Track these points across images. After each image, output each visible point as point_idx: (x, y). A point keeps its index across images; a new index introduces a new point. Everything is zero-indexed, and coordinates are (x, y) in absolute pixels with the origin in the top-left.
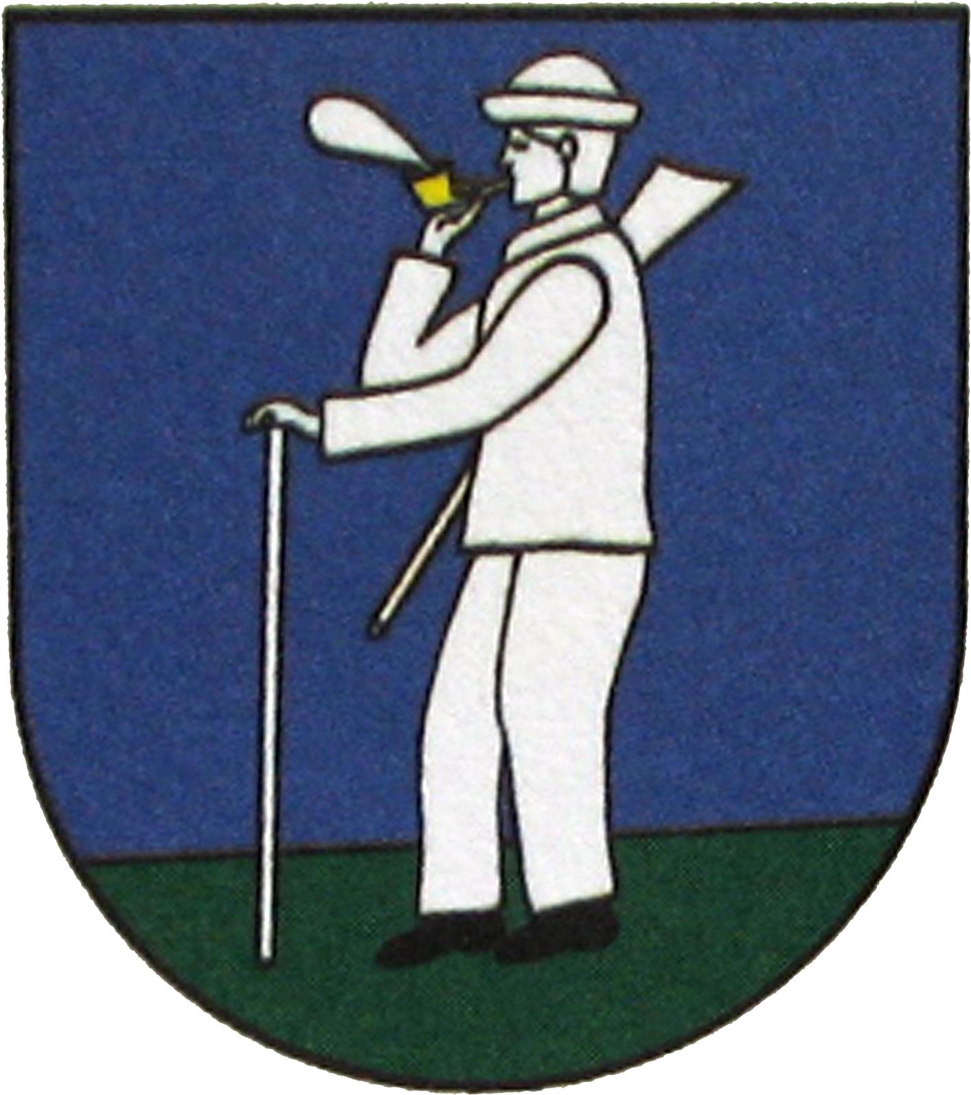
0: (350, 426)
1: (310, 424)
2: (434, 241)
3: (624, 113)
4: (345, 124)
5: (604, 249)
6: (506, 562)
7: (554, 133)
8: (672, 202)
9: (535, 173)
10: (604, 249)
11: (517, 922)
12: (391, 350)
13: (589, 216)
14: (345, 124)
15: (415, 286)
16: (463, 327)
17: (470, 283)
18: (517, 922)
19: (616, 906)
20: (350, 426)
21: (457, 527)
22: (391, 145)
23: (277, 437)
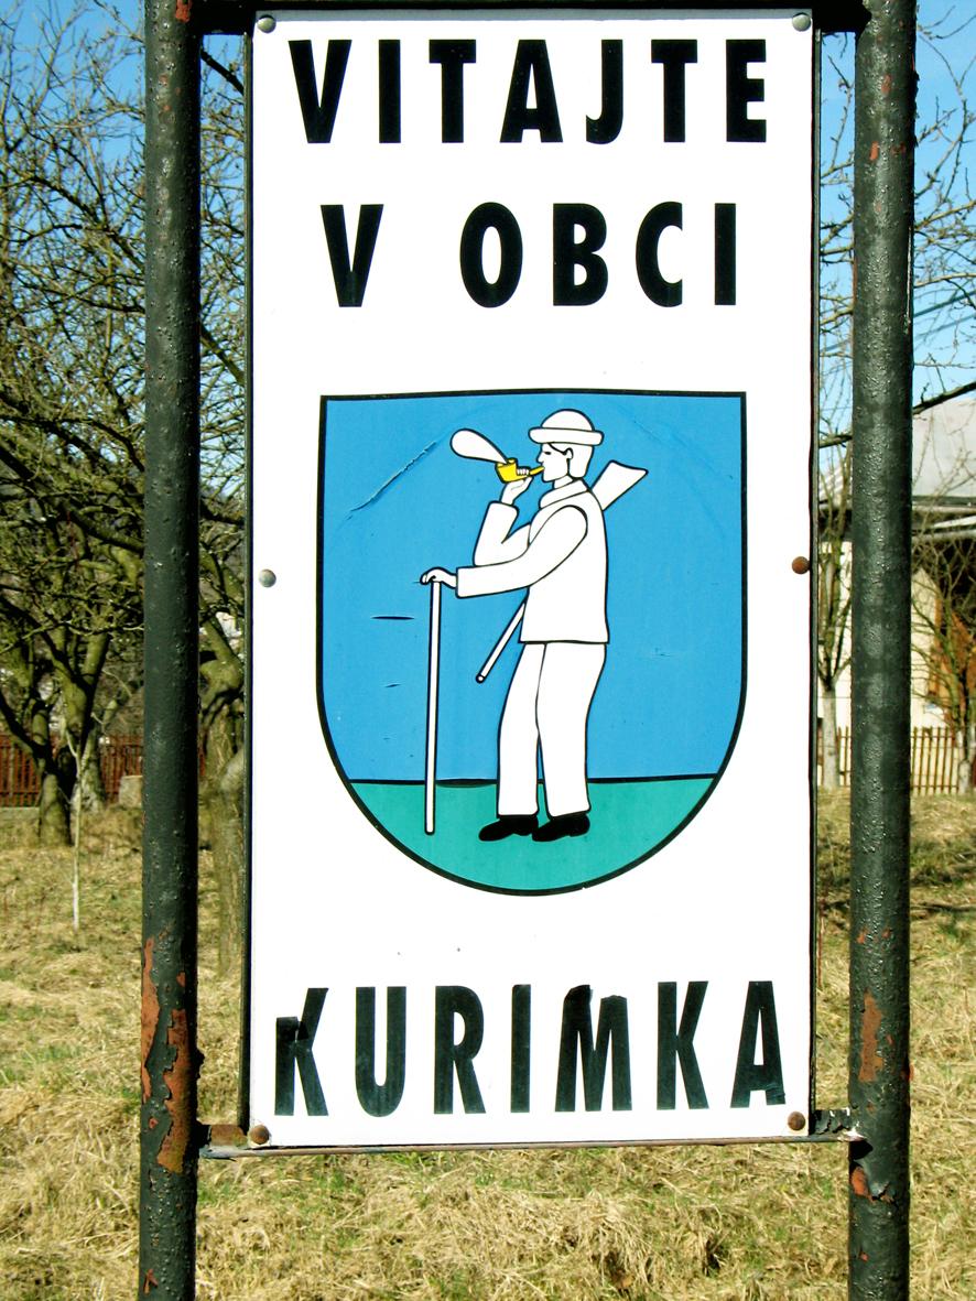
0: (469, 583)
1: (451, 580)
2: (508, 497)
3: (596, 439)
4: (467, 444)
5: (585, 501)
6: (543, 646)
7: (563, 448)
8: (616, 481)
9: (553, 466)
10: (585, 501)
11: (543, 821)
12: (489, 548)
13: (579, 486)
14: (467, 444)
15: (501, 517)
16: (522, 534)
17: (525, 516)
18: (543, 821)
19: (588, 815)
20: (469, 583)
21: (518, 630)
22: (495, 456)
23: (436, 586)
